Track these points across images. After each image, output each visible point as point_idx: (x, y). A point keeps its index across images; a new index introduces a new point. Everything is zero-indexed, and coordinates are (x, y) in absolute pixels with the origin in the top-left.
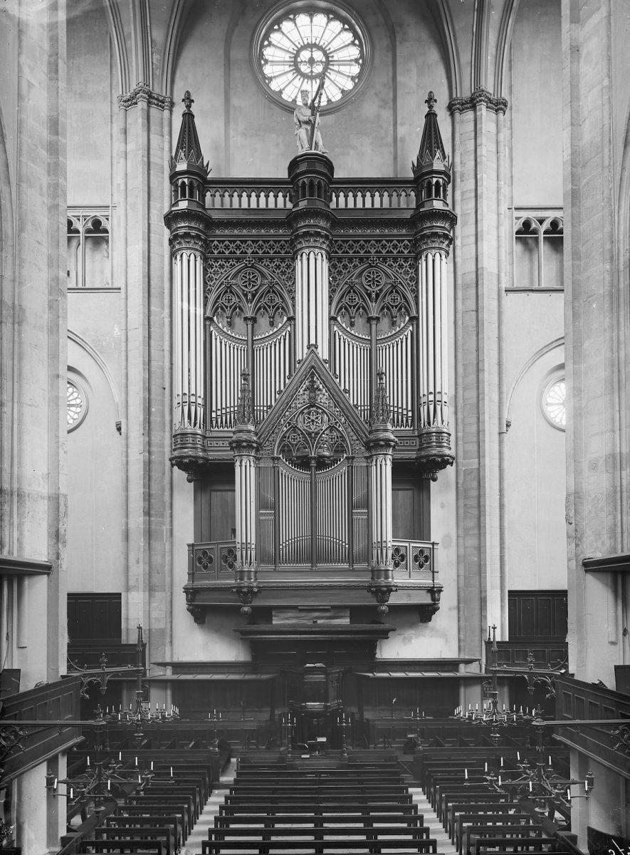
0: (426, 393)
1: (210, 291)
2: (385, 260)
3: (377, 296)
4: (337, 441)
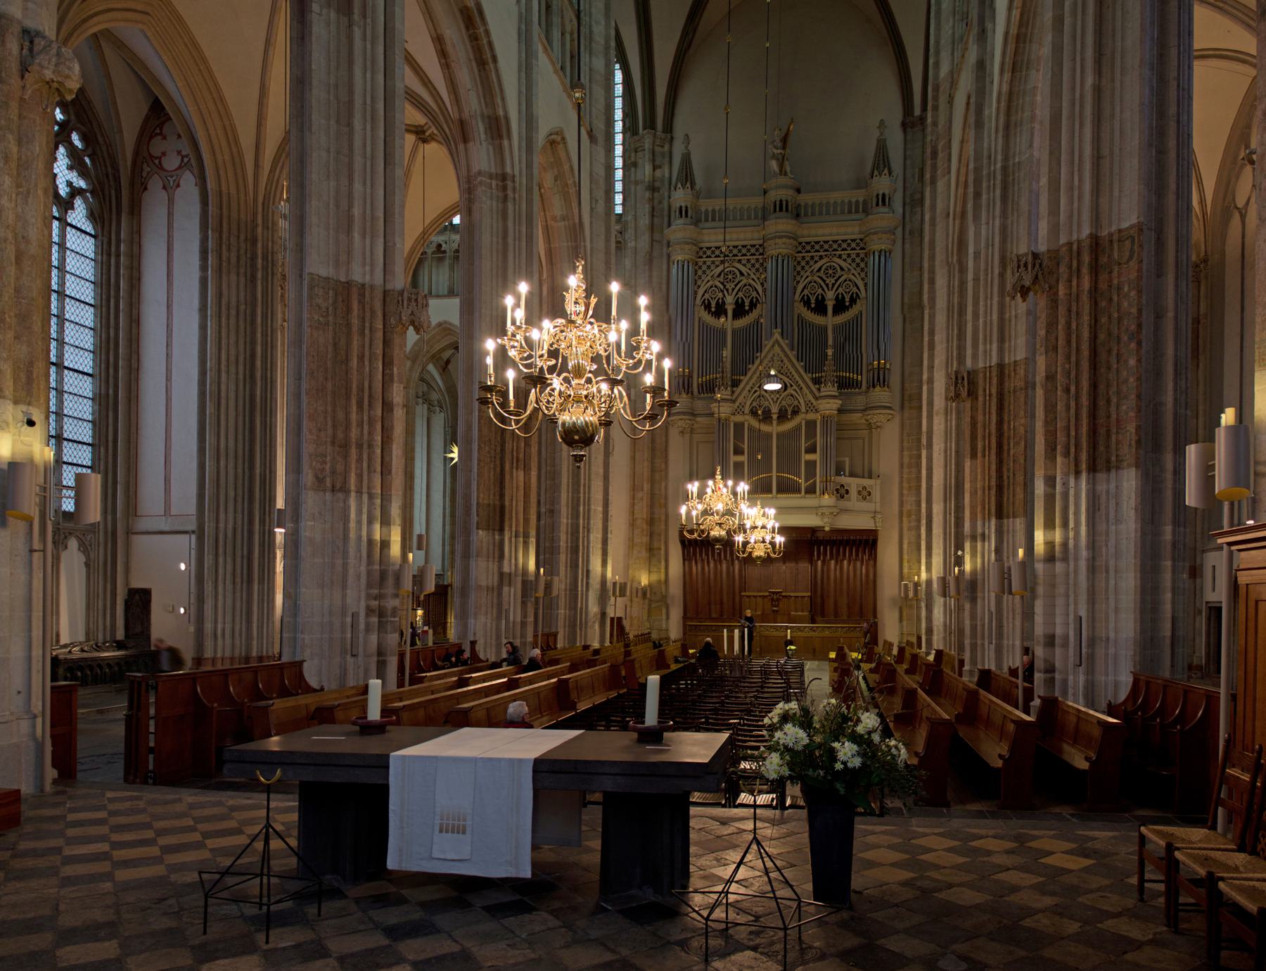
1: (699, 287)
3: (833, 285)
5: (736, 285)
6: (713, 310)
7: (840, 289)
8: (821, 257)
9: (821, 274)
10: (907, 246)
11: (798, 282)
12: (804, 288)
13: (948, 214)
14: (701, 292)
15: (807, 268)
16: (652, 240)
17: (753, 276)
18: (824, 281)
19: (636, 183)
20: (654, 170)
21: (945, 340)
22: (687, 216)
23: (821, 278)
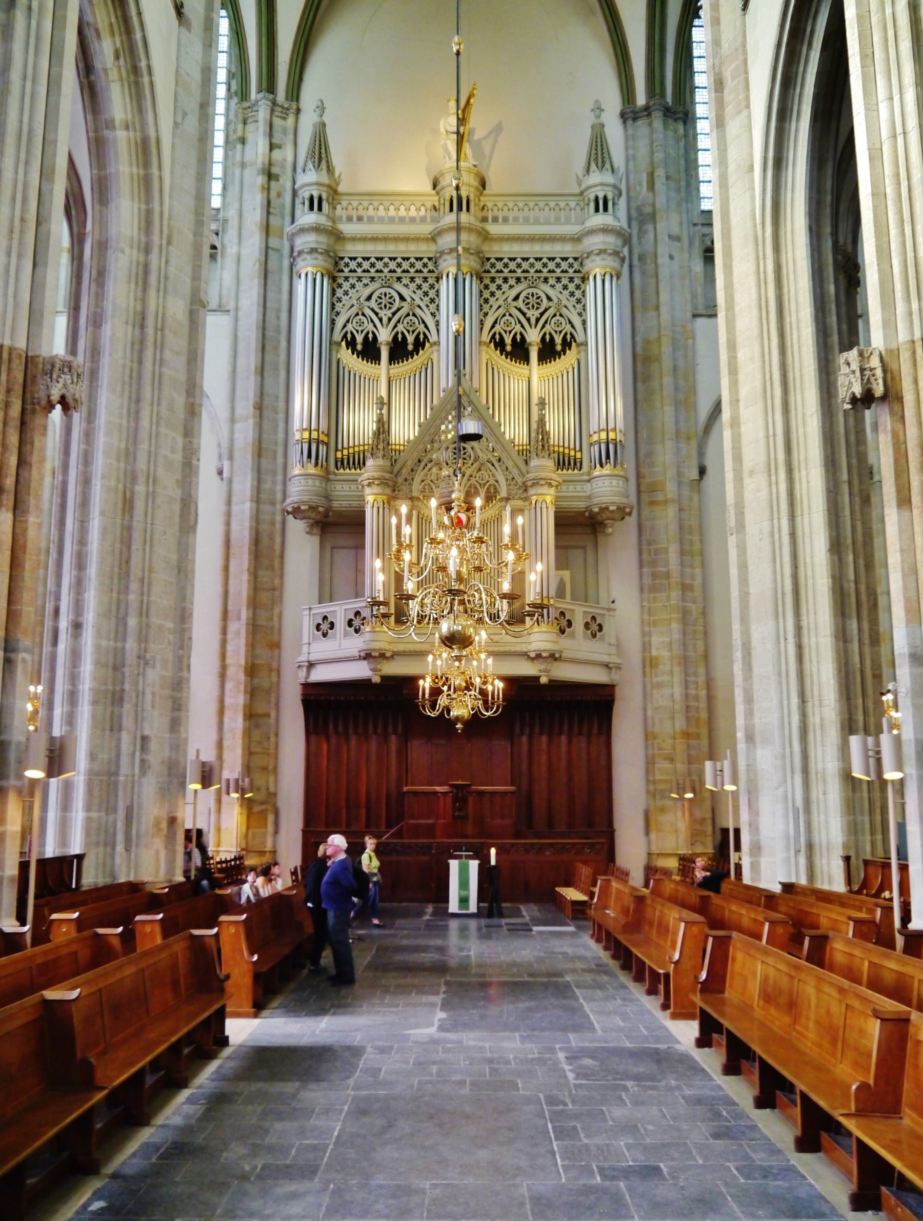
0: (596, 429)
1: (338, 314)
2: (546, 280)
3: (538, 320)
5: (394, 314)
6: (359, 347)
7: (547, 326)
8: (518, 280)
9: (520, 303)
11: (486, 314)
12: (495, 322)
14: (340, 322)
15: (498, 293)
16: (267, 247)
17: (418, 301)
18: (524, 314)
19: (243, 165)
20: (271, 150)
21: (757, 355)
22: (320, 209)
23: (520, 310)
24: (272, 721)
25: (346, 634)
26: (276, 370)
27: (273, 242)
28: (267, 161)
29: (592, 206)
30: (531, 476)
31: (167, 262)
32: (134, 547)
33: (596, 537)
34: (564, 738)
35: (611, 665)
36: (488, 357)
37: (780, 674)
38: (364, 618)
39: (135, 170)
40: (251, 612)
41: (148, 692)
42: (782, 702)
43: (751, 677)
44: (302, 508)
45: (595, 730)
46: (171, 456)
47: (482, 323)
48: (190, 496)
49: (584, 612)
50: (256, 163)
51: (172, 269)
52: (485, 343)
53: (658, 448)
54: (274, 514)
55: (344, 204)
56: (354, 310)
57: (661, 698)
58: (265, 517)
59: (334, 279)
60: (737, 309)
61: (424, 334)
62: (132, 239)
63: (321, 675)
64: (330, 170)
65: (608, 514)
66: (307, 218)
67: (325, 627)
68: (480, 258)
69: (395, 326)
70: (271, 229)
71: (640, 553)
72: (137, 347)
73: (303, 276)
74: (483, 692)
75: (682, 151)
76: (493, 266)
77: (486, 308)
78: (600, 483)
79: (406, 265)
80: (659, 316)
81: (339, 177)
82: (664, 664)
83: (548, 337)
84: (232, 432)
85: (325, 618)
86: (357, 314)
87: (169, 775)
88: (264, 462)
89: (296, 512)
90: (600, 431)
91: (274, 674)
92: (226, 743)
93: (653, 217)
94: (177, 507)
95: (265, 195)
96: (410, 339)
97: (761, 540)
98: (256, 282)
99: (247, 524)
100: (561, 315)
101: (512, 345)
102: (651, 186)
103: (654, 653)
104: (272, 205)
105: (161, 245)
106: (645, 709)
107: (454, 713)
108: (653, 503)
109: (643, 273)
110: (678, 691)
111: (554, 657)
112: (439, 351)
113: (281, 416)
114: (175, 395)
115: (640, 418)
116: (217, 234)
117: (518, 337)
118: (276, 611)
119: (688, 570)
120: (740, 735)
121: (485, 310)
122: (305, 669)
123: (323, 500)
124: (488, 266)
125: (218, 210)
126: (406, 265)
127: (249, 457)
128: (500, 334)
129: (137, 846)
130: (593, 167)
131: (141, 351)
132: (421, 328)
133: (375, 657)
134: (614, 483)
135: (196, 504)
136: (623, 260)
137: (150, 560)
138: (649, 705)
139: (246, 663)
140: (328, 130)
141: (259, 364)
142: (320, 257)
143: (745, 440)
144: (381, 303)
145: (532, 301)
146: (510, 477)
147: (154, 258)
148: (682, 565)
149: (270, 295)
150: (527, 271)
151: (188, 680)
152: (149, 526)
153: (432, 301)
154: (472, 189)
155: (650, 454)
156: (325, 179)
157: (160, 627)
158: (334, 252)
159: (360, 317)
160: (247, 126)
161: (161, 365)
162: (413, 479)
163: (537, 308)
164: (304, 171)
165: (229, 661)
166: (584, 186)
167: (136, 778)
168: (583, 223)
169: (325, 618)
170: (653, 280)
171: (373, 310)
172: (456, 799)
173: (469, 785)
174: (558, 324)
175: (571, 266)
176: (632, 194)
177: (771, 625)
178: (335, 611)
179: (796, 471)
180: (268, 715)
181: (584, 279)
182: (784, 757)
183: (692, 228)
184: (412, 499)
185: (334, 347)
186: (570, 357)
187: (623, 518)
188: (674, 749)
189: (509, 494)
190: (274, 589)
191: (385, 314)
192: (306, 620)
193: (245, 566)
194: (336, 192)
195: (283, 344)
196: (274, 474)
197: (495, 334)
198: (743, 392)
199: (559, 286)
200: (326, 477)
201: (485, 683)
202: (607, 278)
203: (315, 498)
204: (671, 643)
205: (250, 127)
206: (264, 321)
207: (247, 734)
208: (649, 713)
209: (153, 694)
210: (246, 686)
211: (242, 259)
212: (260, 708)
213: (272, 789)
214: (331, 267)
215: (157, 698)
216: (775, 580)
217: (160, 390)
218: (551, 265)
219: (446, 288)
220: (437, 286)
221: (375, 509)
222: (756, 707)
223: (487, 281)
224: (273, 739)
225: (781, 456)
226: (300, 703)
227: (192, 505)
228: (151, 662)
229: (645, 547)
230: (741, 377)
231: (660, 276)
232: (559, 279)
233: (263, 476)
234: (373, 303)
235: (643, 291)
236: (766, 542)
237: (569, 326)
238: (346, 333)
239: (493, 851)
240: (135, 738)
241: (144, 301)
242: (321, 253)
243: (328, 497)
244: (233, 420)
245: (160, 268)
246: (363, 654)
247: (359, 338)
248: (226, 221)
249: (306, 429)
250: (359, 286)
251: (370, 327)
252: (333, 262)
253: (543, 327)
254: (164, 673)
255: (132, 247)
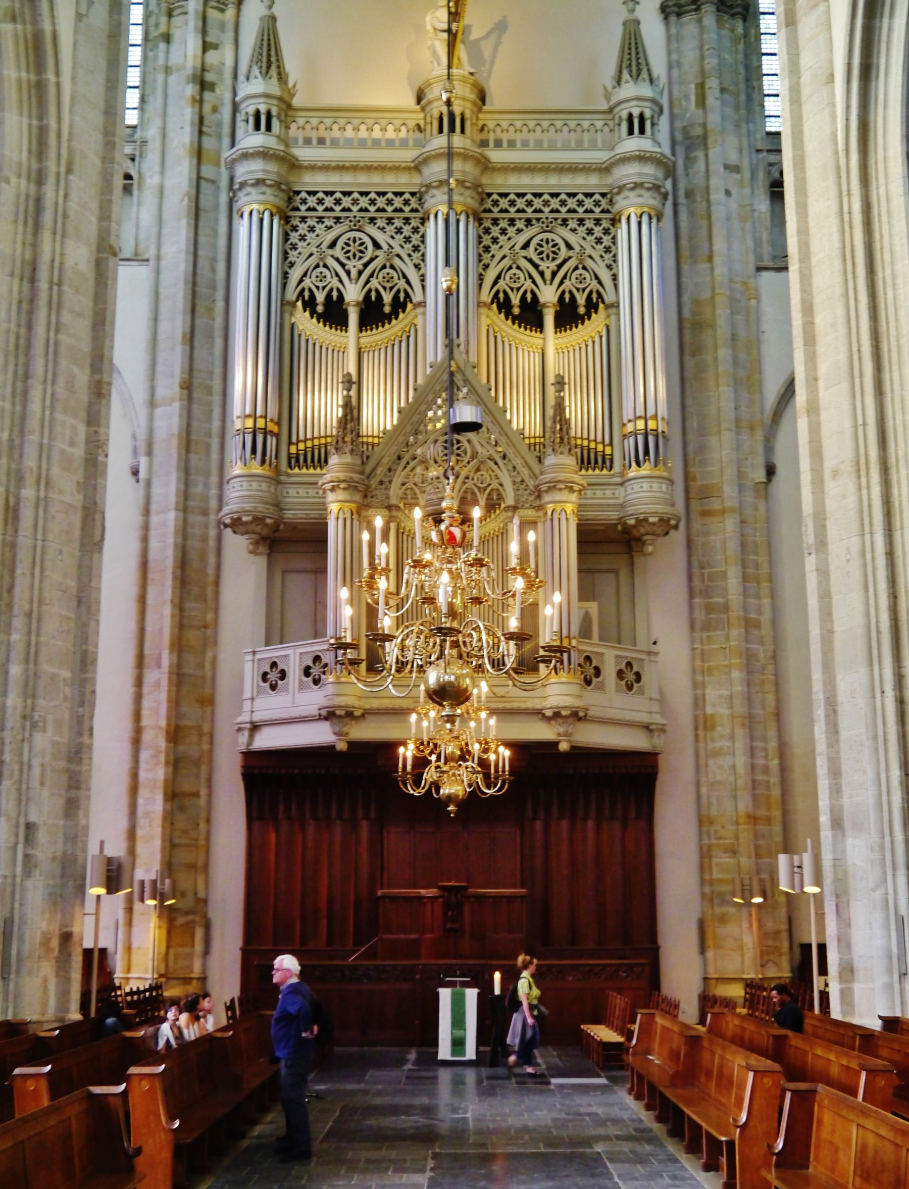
0: (631, 417)
1: (292, 265)
2: (565, 222)
3: (554, 274)
4: (489, 485)
5: (366, 265)
6: (320, 309)
7: (567, 282)
8: (529, 222)
9: (531, 252)
10: (683, 216)
11: (486, 266)
12: (499, 277)
13: (831, 78)
14: (295, 274)
15: (502, 239)
16: (199, 178)
17: (397, 249)
18: (536, 266)
19: (167, 70)
20: (204, 50)
22: (269, 128)
23: (530, 261)
24: (202, 801)
25: (302, 686)
26: (210, 336)
27: (207, 171)
28: (199, 65)
29: (624, 126)
30: (547, 477)
31: (66, 196)
32: (19, 571)
33: (632, 557)
34: (590, 824)
35: (652, 727)
36: (489, 322)
37: (875, 738)
38: (326, 665)
39: (24, 75)
40: (175, 655)
41: (36, 762)
42: (878, 774)
43: (837, 741)
44: (244, 519)
45: (633, 813)
46: (70, 450)
47: (481, 278)
48: (95, 503)
49: (617, 657)
50: (184, 68)
51: (72, 205)
52: (485, 304)
53: (713, 441)
54: (206, 526)
55: (301, 121)
56: (313, 261)
57: (718, 769)
58: (195, 531)
59: (286, 219)
60: (814, 260)
61: (406, 291)
62: (20, 164)
63: (267, 740)
64: (282, 77)
65: (649, 529)
66: (252, 140)
67: (273, 676)
68: (479, 193)
69: (368, 282)
70: (204, 154)
71: (690, 578)
72: (25, 306)
73: (246, 215)
74: (483, 763)
75: (741, 57)
76: (495, 203)
77: (486, 258)
78: (637, 488)
79: (381, 202)
80: (712, 269)
81: (294, 86)
82: (722, 725)
83: (567, 297)
84: (151, 418)
85: (274, 665)
86: (317, 266)
87: (62, 876)
88: (194, 459)
89: (236, 525)
90: (637, 418)
91: (206, 739)
92: (140, 832)
93: (704, 140)
94: (77, 519)
95: (197, 110)
96: (387, 298)
97: (848, 561)
98: (184, 222)
99: (171, 540)
100: (584, 268)
101: (520, 307)
102: (701, 101)
103: (709, 710)
104: (206, 122)
105: (58, 174)
106: (698, 784)
107: (445, 791)
108: (705, 513)
109: (692, 213)
110: (741, 761)
111: (577, 716)
112: (424, 314)
113: (217, 398)
114: (76, 370)
115: (689, 402)
116: (133, 160)
117: (529, 296)
118: (209, 655)
119: (752, 601)
120: (824, 819)
121: (485, 261)
122: (246, 733)
123: (272, 509)
124: (488, 204)
125: (134, 127)
126: (381, 202)
127: (174, 452)
128: (505, 292)
129: (18, 972)
130: (626, 75)
131: (30, 313)
132: (402, 284)
133: (340, 717)
134: (655, 486)
135: (103, 514)
136: (665, 196)
137: (41, 588)
138: (703, 779)
139: (168, 725)
140: (279, 25)
141: (188, 330)
142: (269, 191)
143: (827, 431)
144: (348, 252)
145: (546, 249)
146: (518, 479)
147: (49, 191)
148: (745, 594)
149: (202, 239)
150: (540, 211)
151: (90, 747)
152: (39, 543)
153: (416, 249)
154: (468, 105)
155: (702, 449)
156: (274, 88)
157: (53, 677)
158: (287, 184)
159: (321, 269)
160: (173, 20)
161: (57, 331)
162: (390, 482)
163: (554, 259)
164: (248, 79)
165: (145, 722)
166: (614, 101)
167: (18, 880)
168: (613, 149)
169: (274, 665)
170: (705, 223)
171: (337, 260)
172: (447, 906)
173: (465, 888)
174: (581, 279)
175: (597, 204)
176: (676, 111)
177: (863, 671)
178: (286, 656)
179: (893, 471)
180: (196, 795)
181: (615, 221)
182: (882, 848)
183: (754, 155)
184: (389, 508)
185: (287, 308)
186: (597, 322)
187: (667, 533)
188: (737, 838)
189: (517, 501)
190: (205, 627)
191: (354, 265)
192: (248, 667)
193: (168, 594)
194: (289, 106)
195: (220, 304)
196: (207, 474)
197: (498, 292)
198: (823, 368)
199: (582, 230)
200: (276, 479)
201: (486, 751)
202: (645, 219)
203: (260, 507)
204: (731, 697)
205: (177, 21)
206: (194, 273)
207: (169, 819)
208: (704, 790)
209: (43, 765)
210: (167, 757)
211: (167, 193)
212: (186, 786)
213: (201, 894)
214: (283, 205)
215: (48, 773)
216: (868, 614)
217: (55, 362)
218: (572, 203)
219: (434, 232)
220: (422, 229)
221: (341, 521)
222: (844, 781)
223: (487, 224)
224: (203, 826)
225: (874, 452)
226: (239, 778)
227: (98, 516)
228: (40, 724)
229: (696, 571)
230: (820, 348)
231: (713, 217)
232: (581, 221)
233: (192, 477)
234: (338, 252)
235: (691, 238)
236: (856, 564)
237: (595, 282)
238: (303, 290)
239: (497, 976)
240: (17, 825)
241: (35, 246)
242: (270, 186)
243: (278, 505)
244: (152, 404)
245: (57, 203)
246: (324, 712)
247: (320, 297)
248: (144, 142)
249: (249, 416)
250: (320, 228)
251: (335, 283)
252: (286, 198)
253: (561, 283)
254: (57, 739)
255: (19, 176)
